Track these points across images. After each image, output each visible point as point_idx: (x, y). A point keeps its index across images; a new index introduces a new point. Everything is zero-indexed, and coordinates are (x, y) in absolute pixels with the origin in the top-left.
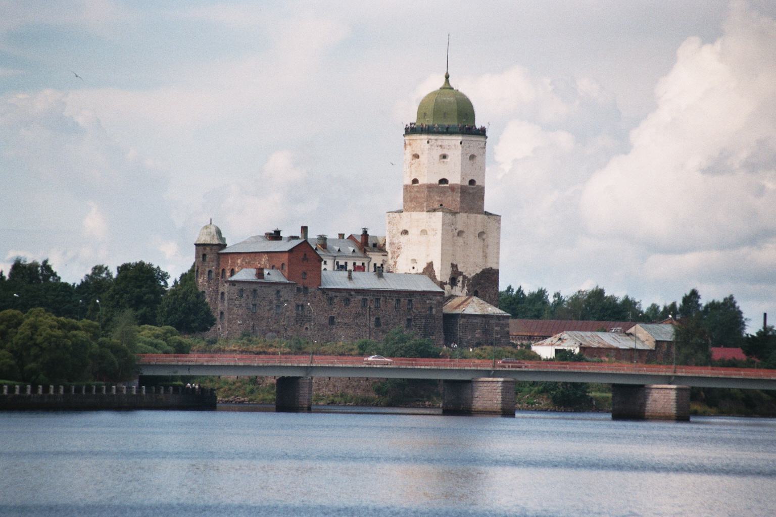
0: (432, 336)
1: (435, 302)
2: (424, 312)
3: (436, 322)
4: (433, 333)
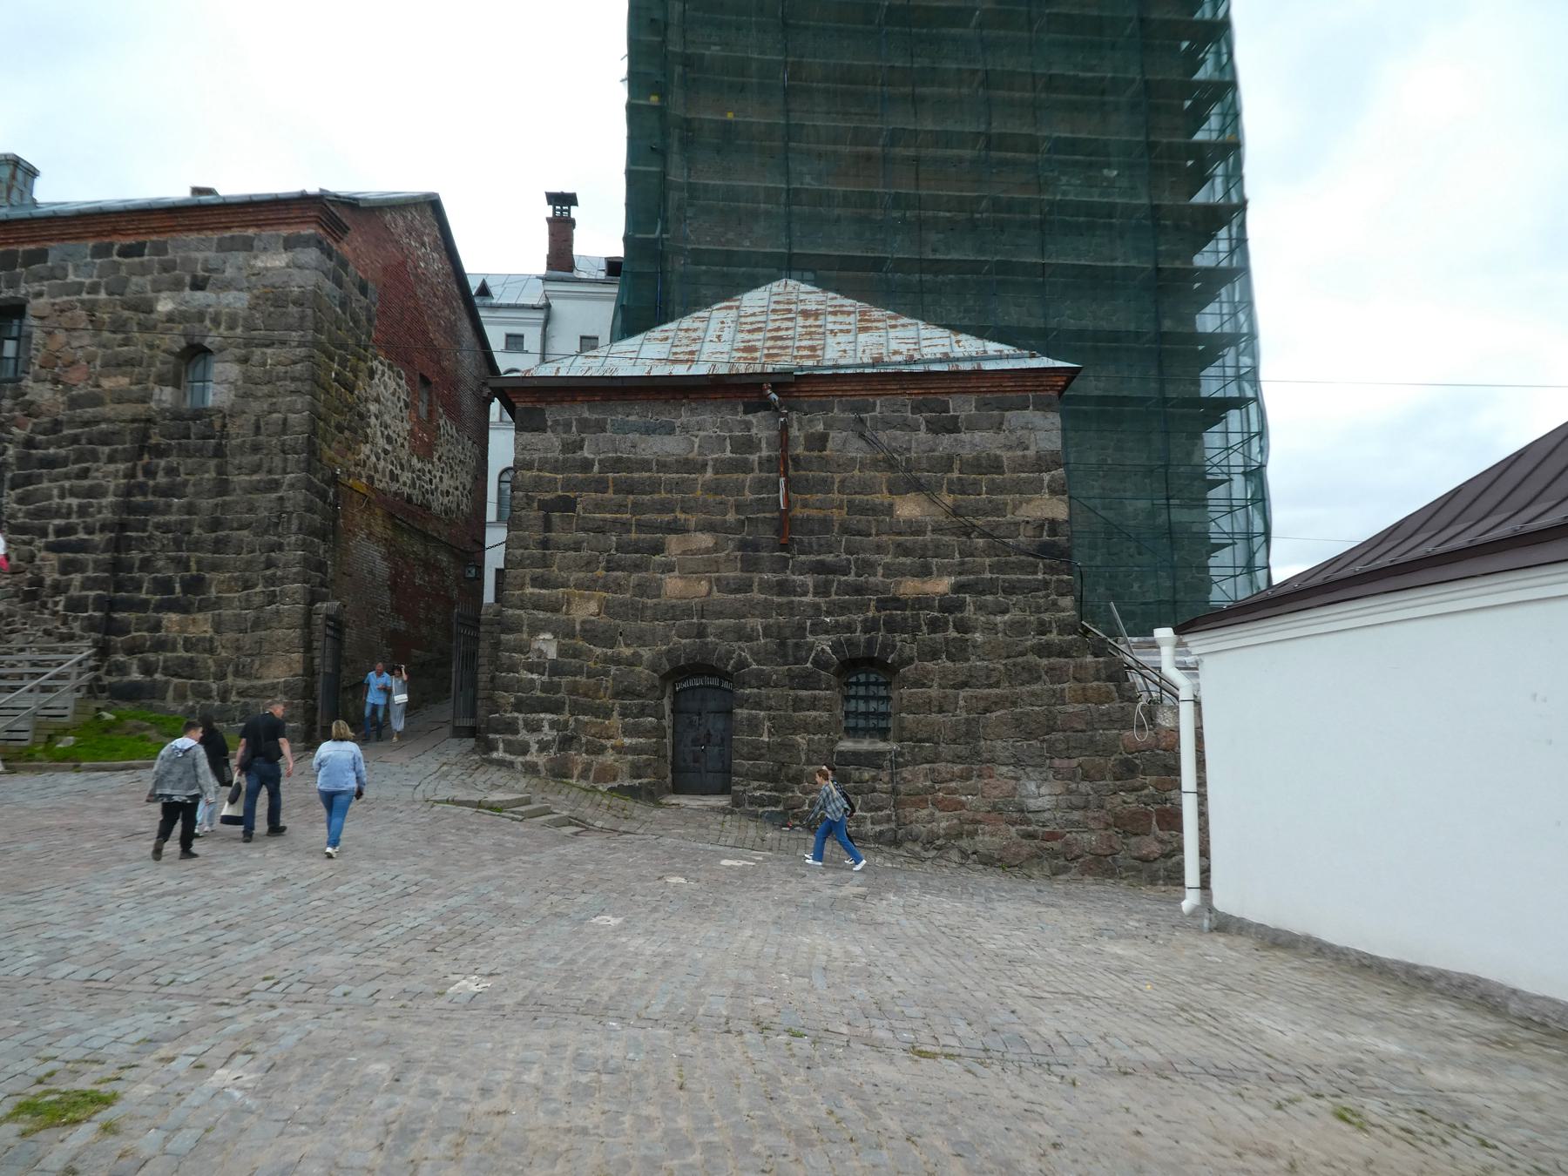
0: (184, 609)
1: (236, 301)
2: (120, 398)
3: (239, 479)
4: (195, 585)
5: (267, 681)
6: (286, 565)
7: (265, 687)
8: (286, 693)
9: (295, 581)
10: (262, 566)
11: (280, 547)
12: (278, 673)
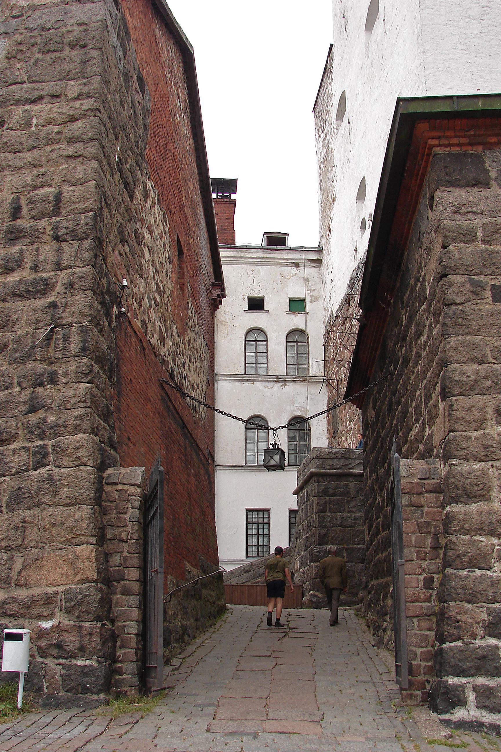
5: (36, 591)
6: (63, 406)
7: (32, 602)
8: (69, 611)
9: (77, 429)
10: (24, 408)
11: (53, 380)
12: (54, 576)
